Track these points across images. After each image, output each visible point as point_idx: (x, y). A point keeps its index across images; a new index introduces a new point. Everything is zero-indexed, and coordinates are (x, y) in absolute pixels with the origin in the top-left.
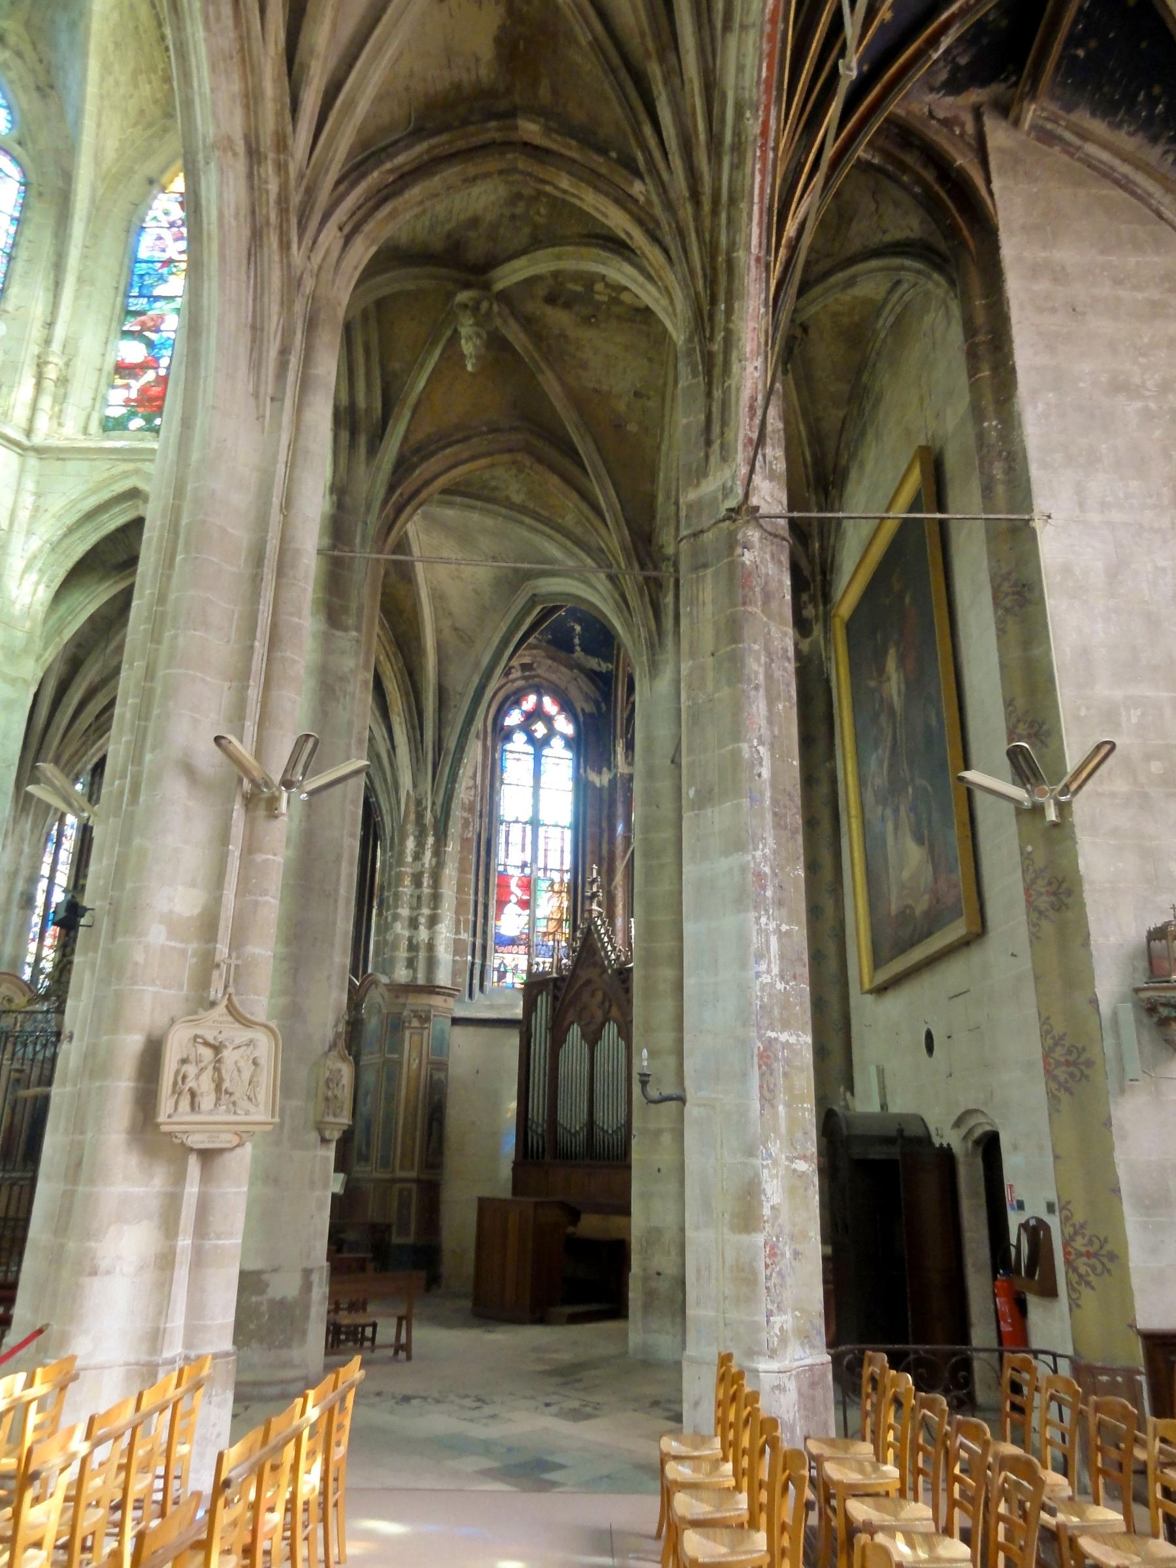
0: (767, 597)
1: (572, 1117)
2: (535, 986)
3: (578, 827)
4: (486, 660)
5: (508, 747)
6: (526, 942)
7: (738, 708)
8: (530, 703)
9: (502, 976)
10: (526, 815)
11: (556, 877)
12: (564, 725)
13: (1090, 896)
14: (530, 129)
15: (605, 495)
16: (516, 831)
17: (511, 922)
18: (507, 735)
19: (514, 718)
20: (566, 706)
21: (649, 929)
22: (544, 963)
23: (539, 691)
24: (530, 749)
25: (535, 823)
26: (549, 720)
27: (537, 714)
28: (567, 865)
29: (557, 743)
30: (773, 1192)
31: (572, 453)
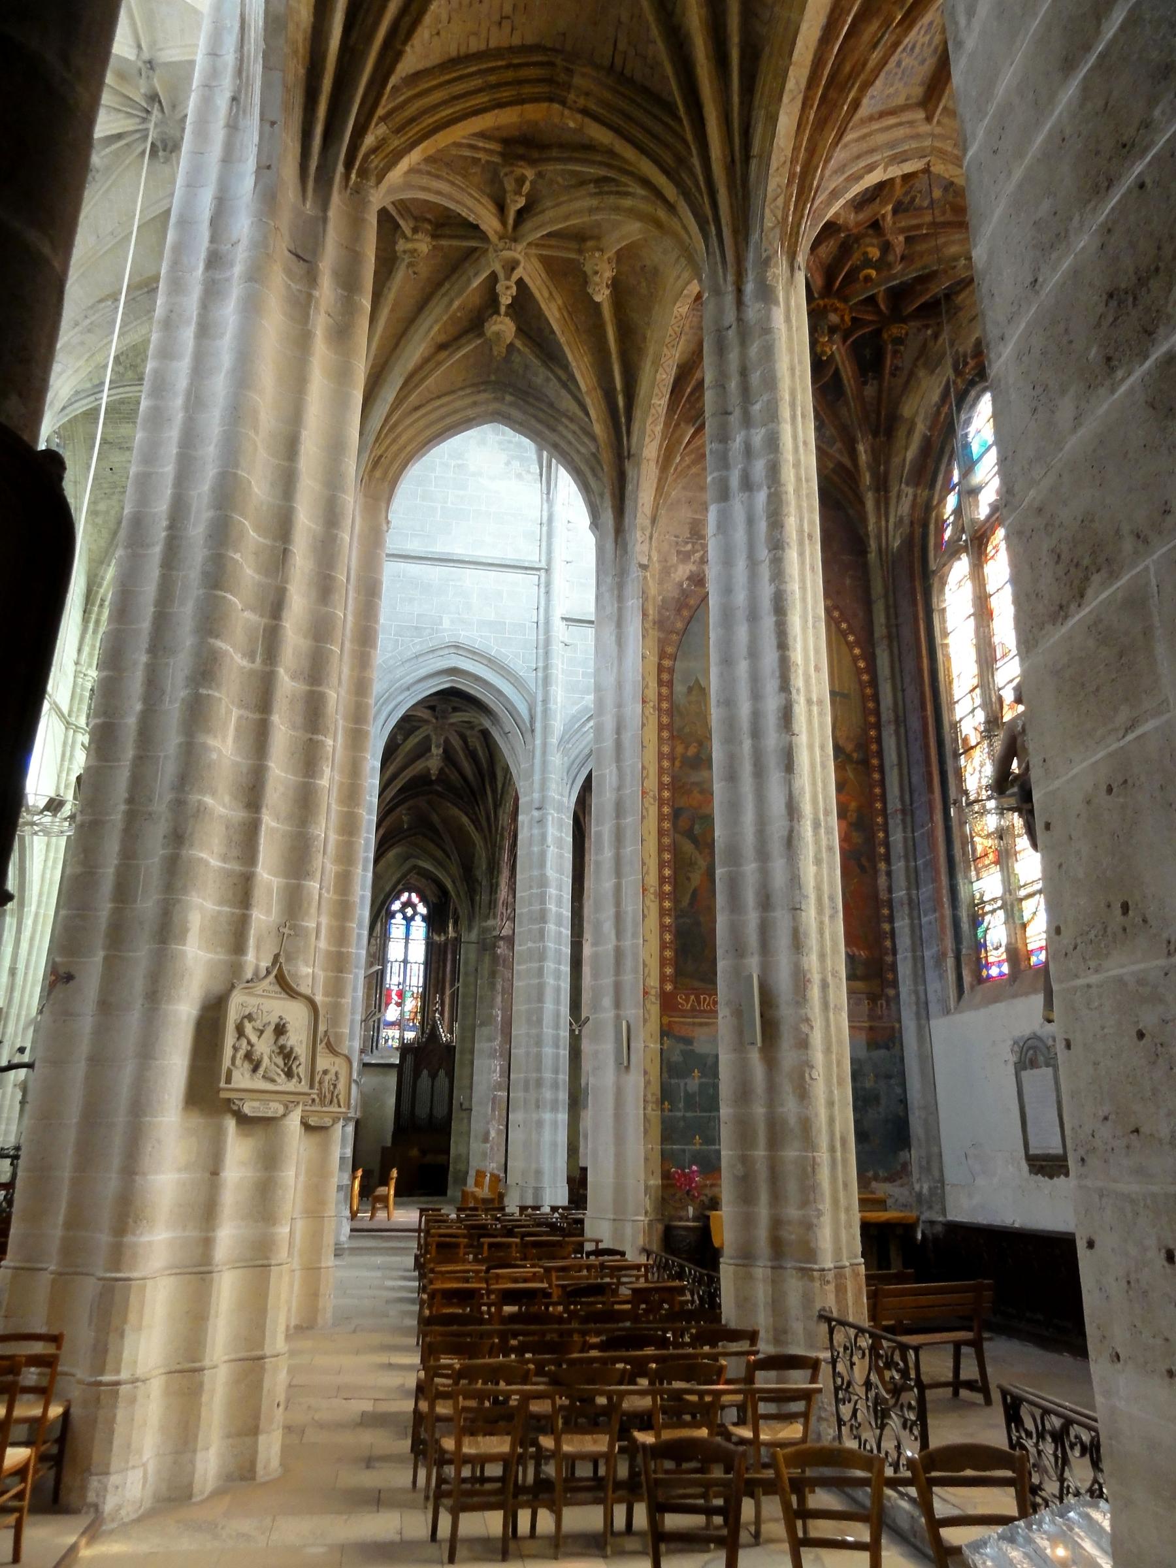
0: (504, 961)
1: (422, 1112)
2: (405, 1049)
3: (428, 963)
4: (388, 888)
5: (393, 921)
6: (398, 1024)
7: (493, 999)
8: (405, 897)
9: (386, 1041)
10: (401, 958)
12: (422, 909)
14: (439, 789)
15: (455, 856)
16: (396, 965)
17: (392, 1014)
18: (392, 915)
19: (396, 906)
20: (423, 899)
21: (463, 1039)
22: (410, 1035)
24: (404, 922)
25: (405, 962)
26: (414, 906)
27: (408, 904)
28: (421, 984)
29: (418, 918)
30: (493, 1134)
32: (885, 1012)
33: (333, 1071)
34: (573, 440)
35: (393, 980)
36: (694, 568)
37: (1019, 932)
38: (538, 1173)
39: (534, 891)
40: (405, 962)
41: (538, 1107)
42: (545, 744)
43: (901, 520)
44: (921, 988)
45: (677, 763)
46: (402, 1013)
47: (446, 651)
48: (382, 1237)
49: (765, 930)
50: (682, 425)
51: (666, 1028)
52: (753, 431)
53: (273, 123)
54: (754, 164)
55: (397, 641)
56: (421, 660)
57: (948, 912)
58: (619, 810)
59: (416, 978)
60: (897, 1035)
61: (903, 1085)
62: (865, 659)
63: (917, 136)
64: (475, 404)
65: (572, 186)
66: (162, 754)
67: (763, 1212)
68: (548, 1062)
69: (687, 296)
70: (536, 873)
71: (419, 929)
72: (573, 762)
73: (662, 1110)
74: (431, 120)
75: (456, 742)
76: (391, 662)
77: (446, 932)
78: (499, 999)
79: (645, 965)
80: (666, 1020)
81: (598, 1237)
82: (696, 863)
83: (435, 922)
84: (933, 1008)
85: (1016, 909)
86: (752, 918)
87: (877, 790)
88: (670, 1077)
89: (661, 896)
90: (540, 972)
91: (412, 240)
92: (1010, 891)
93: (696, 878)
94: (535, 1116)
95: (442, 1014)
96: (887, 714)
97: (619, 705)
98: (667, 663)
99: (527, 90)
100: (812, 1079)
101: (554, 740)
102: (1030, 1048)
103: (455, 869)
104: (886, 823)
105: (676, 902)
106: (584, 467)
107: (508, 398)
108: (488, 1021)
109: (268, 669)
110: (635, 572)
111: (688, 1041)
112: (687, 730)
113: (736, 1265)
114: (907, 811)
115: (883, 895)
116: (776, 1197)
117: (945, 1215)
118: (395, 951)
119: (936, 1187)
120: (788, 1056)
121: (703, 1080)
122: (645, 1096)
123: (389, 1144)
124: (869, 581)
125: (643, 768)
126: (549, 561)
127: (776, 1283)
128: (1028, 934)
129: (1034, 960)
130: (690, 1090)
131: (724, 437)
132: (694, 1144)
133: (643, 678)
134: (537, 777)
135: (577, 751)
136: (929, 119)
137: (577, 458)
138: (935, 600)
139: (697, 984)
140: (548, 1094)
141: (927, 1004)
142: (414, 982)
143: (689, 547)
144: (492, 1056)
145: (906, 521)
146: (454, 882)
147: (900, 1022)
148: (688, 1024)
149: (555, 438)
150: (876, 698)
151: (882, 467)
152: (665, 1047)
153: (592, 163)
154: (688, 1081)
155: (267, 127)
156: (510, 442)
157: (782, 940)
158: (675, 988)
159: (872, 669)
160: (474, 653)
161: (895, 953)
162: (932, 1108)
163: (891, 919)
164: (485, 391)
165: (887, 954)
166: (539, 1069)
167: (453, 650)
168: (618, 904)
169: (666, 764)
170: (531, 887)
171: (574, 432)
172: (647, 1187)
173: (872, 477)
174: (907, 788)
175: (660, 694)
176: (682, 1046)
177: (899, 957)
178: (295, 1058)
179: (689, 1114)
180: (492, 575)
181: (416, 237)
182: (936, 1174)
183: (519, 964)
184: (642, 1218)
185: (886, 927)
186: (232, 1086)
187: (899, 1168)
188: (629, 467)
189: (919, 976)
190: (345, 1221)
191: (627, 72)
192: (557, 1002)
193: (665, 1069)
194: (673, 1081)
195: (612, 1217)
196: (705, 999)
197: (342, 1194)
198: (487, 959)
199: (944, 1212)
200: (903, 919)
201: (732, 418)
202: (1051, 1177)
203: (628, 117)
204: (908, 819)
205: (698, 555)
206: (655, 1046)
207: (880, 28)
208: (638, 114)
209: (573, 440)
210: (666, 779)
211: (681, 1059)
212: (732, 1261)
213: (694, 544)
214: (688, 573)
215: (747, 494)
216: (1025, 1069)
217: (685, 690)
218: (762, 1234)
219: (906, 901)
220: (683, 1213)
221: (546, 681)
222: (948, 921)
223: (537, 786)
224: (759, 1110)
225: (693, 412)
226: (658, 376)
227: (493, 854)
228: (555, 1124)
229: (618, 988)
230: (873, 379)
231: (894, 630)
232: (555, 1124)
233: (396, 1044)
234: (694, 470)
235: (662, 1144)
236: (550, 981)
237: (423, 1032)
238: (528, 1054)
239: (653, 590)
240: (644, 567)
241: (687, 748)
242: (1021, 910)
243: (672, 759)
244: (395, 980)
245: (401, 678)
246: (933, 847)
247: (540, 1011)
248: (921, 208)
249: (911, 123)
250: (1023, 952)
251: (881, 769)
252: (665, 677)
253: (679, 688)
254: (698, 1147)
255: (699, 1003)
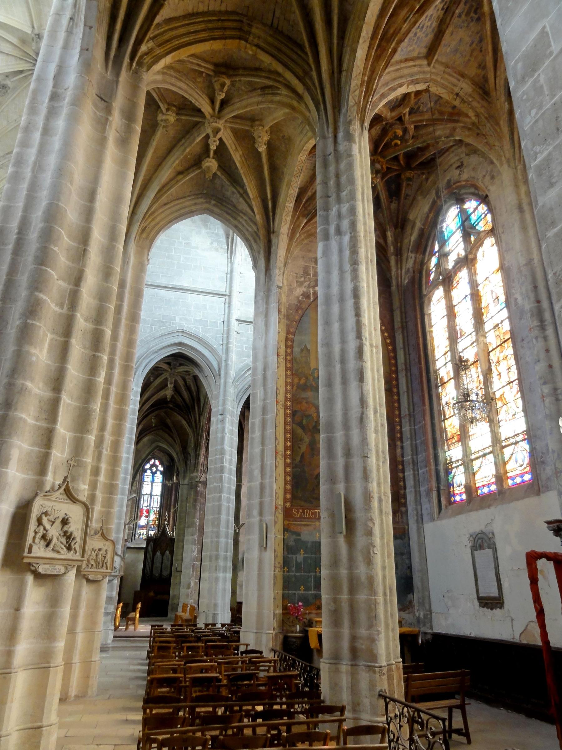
0: (201, 494)
1: (156, 572)
2: (149, 540)
3: (162, 496)
4: (144, 457)
5: (146, 474)
6: (146, 527)
7: (195, 513)
8: (152, 462)
9: (140, 535)
10: (149, 493)
11: (155, 509)
12: (161, 468)
13: (240, 544)
14: (171, 406)
15: (178, 440)
16: (146, 496)
17: (143, 521)
19: (147, 466)
20: (161, 463)
21: (179, 535)
22: (152, 533)
23: (155, 458)
24: (151, 475)
25: (151, 495)
26: (157, 467)
27: (154, 465)
28: (158, 506)
29: (158, 473)
30: (192, 584)
31: (170, 430)
32: (400, 520)
33: (104, 549)
34: (245, 224)
35: (144, 504)
36: (305, 290)
37: (471, 477)
38: (215, 605)
39: (218, 457)
40: (151, 495)
41: (216, 570)
42: (225, 382)
43: (408, 270)
44: (419, 507)
45: (295, 388)
46: (148, 521)
47: (177, 334)
48: (131, 641)
49: (347, 468)
50: (301, 218)
51: (286, 527)
52: (342, 205)
53: (91, 28)
54: (344, 74)
55: (152, 328)
56: (164, 337)
57: (433, 467)
58: (264, 410)
59: (156, 503)
60: (407, 532)
61: (410, 559)
62: (390, 338)
63: (424, 72)
64: (196, 204)
65: (249, 91)
66: (3, 358)
67: (346, 632)
68: (222, 546)
69: (306, 150)
70: (219, 447)
71: (159, 478)
72: (239, 392)
73: (284, 572)
74: (177, 42)
75: (181, 382)
76: (149, 338)
77: (172, 480)
78: (198, 514)
79: (276, 493)
80: (286, 523)
81: (247, 642)
82: (303, 440)
83: (167, 474)
84: (425, 518)
85: (470, 465)
86: (340, 462)
87: (396, 405)
88: (288, 553)
89: (285, 456)
90: (220, 499)
91: (166, 115)
92: (467, 456)
93: (304, 448)
94: (215, 575)
95: (169, 522)
96: (401, 366)
97: (266, 357)
98: (290, 336)
99: (228, 33)
100: (374, 553)
101: (230, 380)
102: (479, 539)
103: (178, 448)
104: (400, 422)
105: (293, 459)
106: (250, 238)
107: (213, 202)
108: (192, 525)
109: (71, 313)
110: (275, 290)
111: (299, 534)
112: (300, 371)
113: (330, 664)
114: (411, 415)
115: (399, 459)
116: (354, 622)
117: (432, 630)
118: (146, 489)
119: (427, 615)
120: (360, 540)
121: (305, 555)
122: (275, 564)
123: (139, 589)
124: (392, 300)
125: (277, 389)
126: (231, 291)
127: (353, 674)
128: (476, 479)
129: (479, 492)
130: (299, 560)
131: (327, 209)
132: (301, 590)
133: (278, 343)
134: (221, 398)
135: (241, 387)
136: (429, 65)
137: (247, 233)
138: (425, 309)
139: (303, 503)
140: (221, 563)
141: (422, 515)
142: (155, 505)
143: (303, 279)
144: (193, 543)
145: (411, 270)
146: (177, 454)
147: (408, 525)
148: (298, 525)
149: (235, 222)
150: (395, 358)
151: (399, 244)
152: (286, 537)
153: (260, 77)
154: (298, 556)
155: (88, 28)
156: (213, 233)
157: (357, 474)
158: (292, 505)
159: (393, 343)
160: (191, 335)
161: (405, 488)
162: (425, 572)
163: (403, 471)
164: (201, 198)
165: (401, 489)
166: (217, 550)
167: (180, 334)
168: (262, 460)
169: (289, 388)
170: (216, 455)
171: (246, 221)
172: (274, 614)
173: (394, 248)
174: (412, 404)
175: (286, 352)
176: (294, 537)
177: (408, 491)
178: (73, 539)
179: (298, 574)
180: (202, 297)
181: (168, 113)
182: (427, 607)
183: (208, 495)
184: (272, 632)
185: (401, 475)
186: (32, 555)
187: (408, 603)
188: (273, 238)
189: (418, 501)
190: (110, 632)
191: (280, 28)
192: (228, 514)
193: (285, 550)
194: (290, 556)
195: (255, 631)
196: (307, 512)
197: (109, 617)
198: (192, 493)
199: (431, 628)
200: (410, 471)
201: (331, 199)
202: (492, 609)
203: (279, 50)
204: (412, 419)
205: (307, 283)
206: (280, 537)
207: (408, 12)
208: (284, 48)
209: (245, 224)
210: (289, 396)
211: (294, 544)
212: (327, 661)
213: (305, 278)
214: (302, 292)
215: (339, 236)
216: (476, 550)
217: (299, 350)
218: (345, 644)
219: (411, 462)
220: (293, 629)
221: (227, 351)
222: (433, 473)
223: (221, 403)
224: (344, 572)
225: (306, 212)
226: (289, 191)
227: (198, 440)
228: (225, 579)
229: (261, 505)
230: (396, 200)
231: (404, 324)
232: (225, 579)
233: (144, 537)
234: (306, 241)
235: (283, 590)
236: (225, 503)
237: (158, 531)
238: (212, 542)
239: (284, 299)
240: (280, 288)
241: (300, 380)
242: (472, 466)
243: (292, 386)
244: (145, 504)
245: (153, 347)
246: (425, 434)
247: (219, 519)
248: (422, 112)
249: (420, 66)
250: (474, 488)
251: (398, 394)
252: (289, 343)
253: (296, 349)
254: (302, 592)
255: (304, 513)
